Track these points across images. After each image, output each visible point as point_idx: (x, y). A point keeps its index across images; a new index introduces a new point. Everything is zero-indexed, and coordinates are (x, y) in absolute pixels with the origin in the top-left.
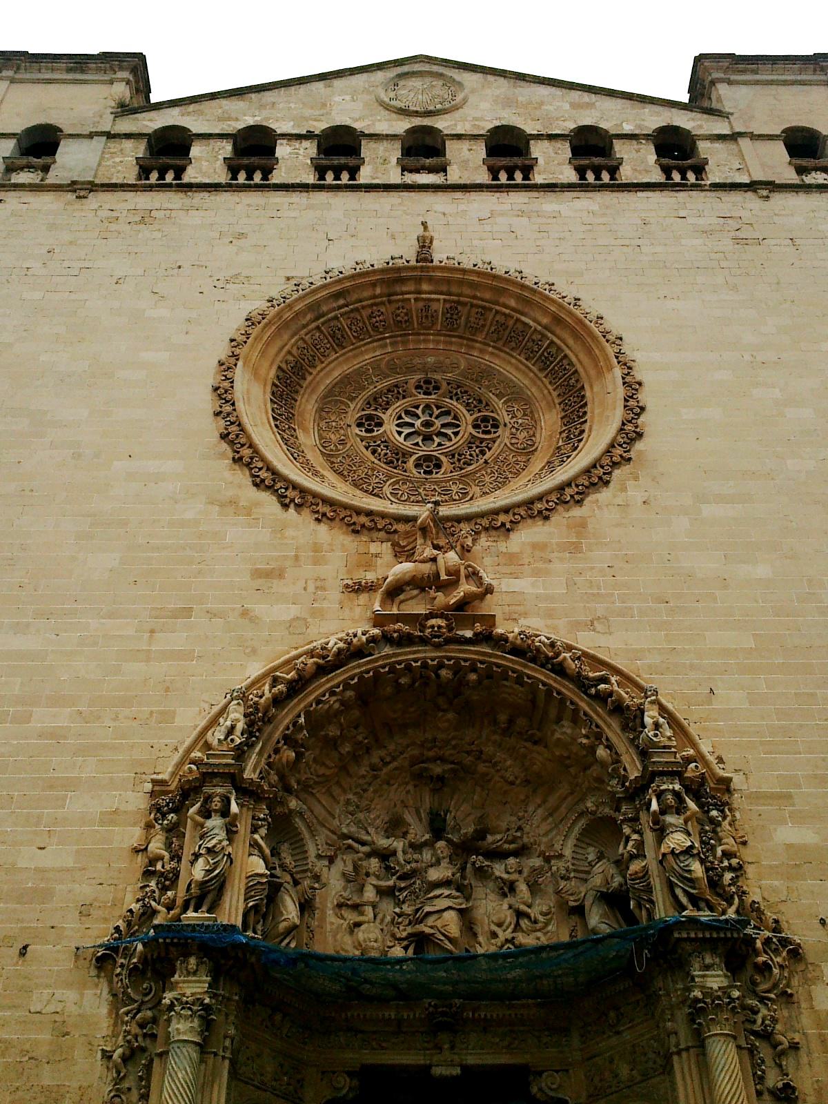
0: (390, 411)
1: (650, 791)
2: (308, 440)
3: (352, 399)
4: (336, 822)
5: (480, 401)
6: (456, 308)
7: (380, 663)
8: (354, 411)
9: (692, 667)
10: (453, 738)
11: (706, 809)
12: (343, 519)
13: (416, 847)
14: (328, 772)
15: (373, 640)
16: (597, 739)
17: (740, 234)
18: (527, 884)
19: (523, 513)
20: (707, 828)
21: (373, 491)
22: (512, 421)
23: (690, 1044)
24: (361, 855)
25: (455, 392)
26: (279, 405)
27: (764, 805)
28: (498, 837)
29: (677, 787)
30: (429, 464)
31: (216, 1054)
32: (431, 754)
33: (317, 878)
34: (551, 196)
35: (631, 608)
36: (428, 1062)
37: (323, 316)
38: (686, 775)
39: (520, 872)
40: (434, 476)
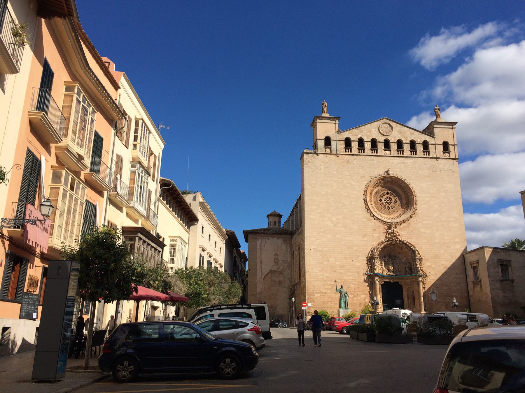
0: (383, 198)
2: (373, 203)
17: (433, 169)
30: (389, 208)
34: (407, 158)
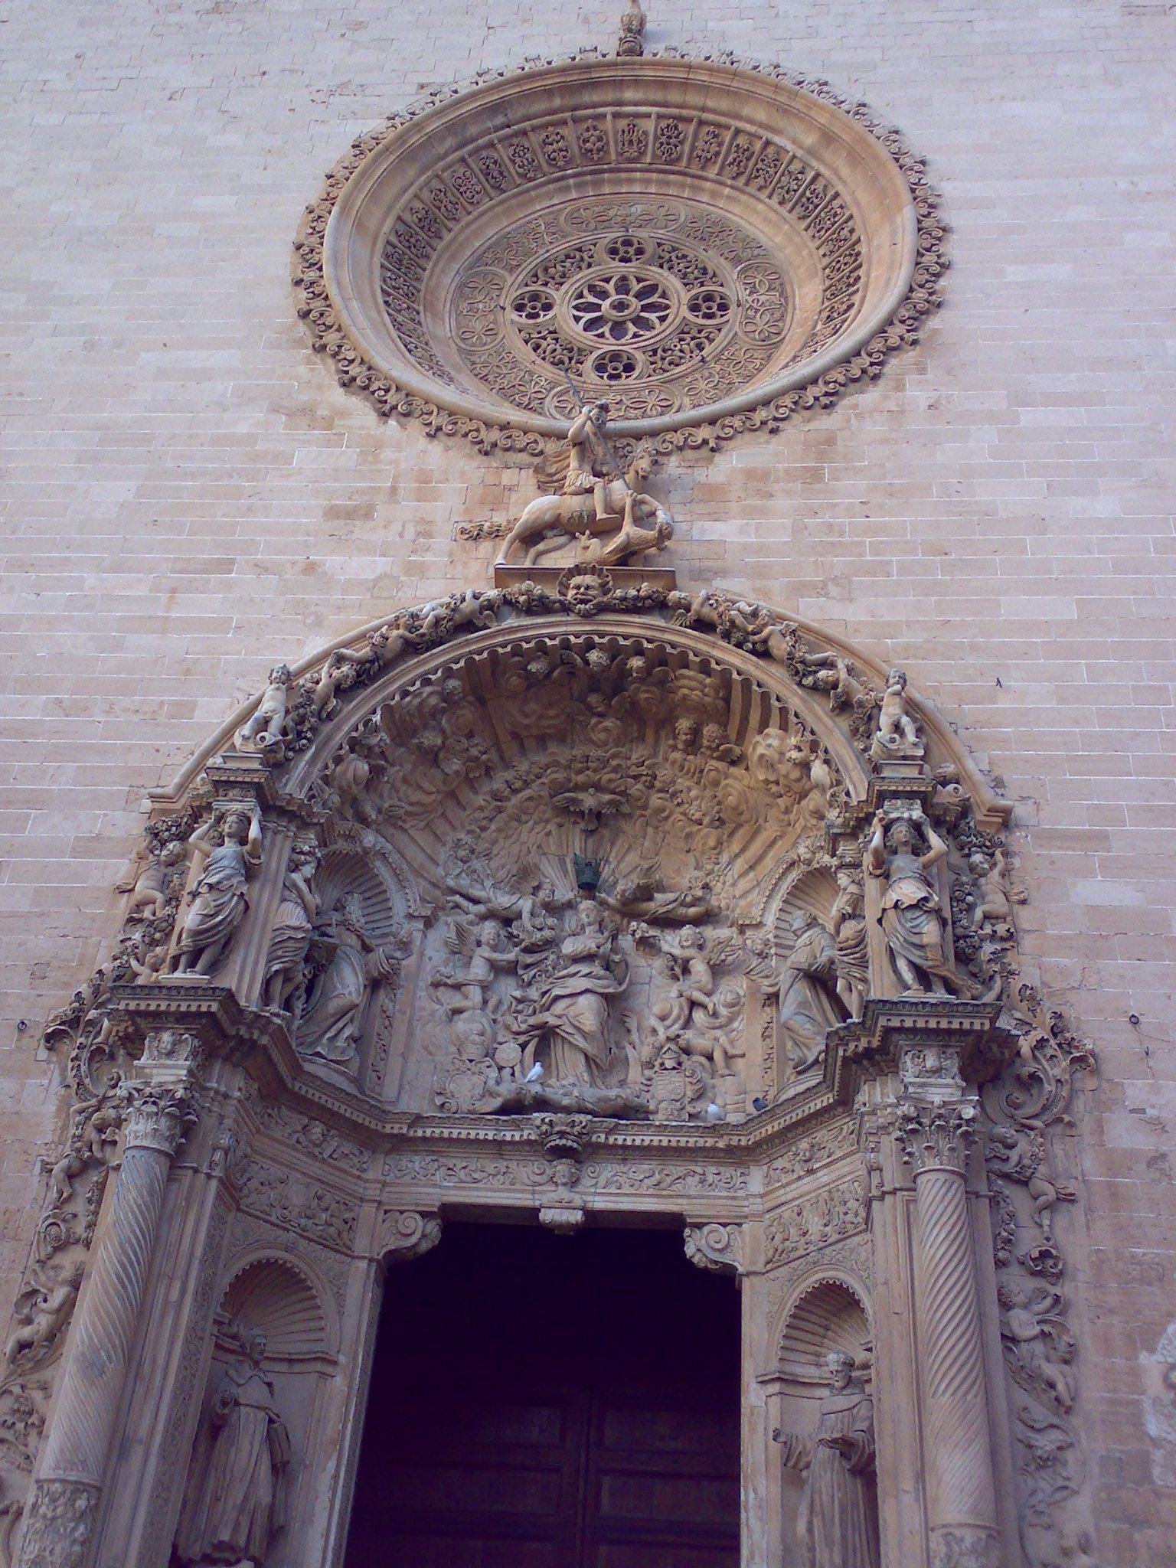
1: (875, 820)
3: (511, 270)
4: (440, 871)
5: (705, 271)
6: (676, 128)
7: (500, 639)
8: (513, 286)
9: (973, 647)
10: (614, 756)
11: (966, 851)
12: (466, 435)
13: (554, 909)
14: (427, 799)
15: (490, 606)
16: (812, 751)
18: (708, 963)
19: (737, 423)
20: (964, 879)
21: (529, 404)
22: (750, 299)
23: (898, 1186)
24: (471, 917)
25: (667, 256)
26: (394, 273)
27: (1060, 848)
28: (671, 896)
29: (917, 814)
31: (196, 1171)
32: (581, 778)
33: (405, 946)
35: (889, 563)
36: (537, 1203)
37: (472, 141)
38: (935, 800)
39: (701, 947)
40: (623, 381)
